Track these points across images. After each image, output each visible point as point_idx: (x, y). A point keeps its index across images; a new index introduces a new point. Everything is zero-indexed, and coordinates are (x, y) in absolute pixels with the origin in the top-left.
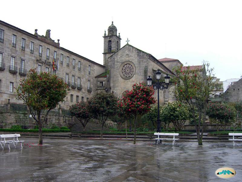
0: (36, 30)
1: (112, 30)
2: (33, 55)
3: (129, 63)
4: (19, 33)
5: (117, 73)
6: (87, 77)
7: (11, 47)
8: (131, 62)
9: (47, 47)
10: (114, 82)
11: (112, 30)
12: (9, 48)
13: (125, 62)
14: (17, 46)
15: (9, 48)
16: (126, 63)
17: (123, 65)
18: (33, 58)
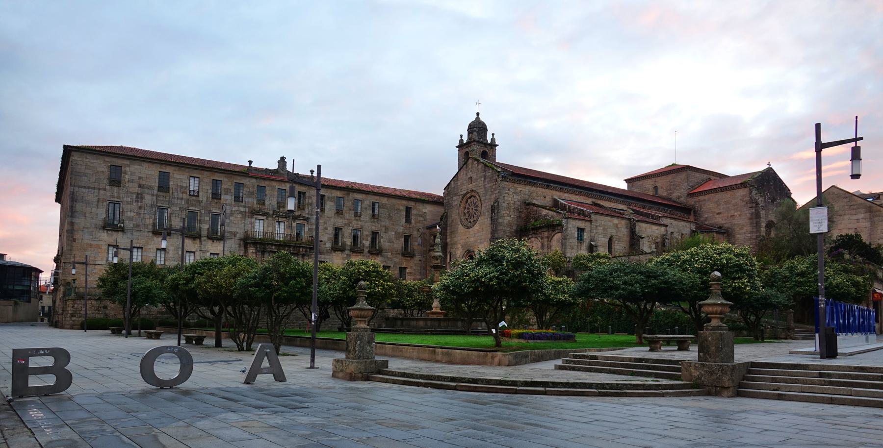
0: (250, 162)
1: (478, 128)
2: (243, 204)
3: (473, 194)
4: (206, 173)
5: (455, 215)
6: (401, 229)
7: (185, 196)
8: (473, 191)
9: (277, 187)
10: (451, 235)
11: (478, 128)
12: (182, 199)
13: (467, 193)
14: (201, 194)
15: (182, 199)
16: (468, 195)
17: (464, 200)
18: (242, 209)
